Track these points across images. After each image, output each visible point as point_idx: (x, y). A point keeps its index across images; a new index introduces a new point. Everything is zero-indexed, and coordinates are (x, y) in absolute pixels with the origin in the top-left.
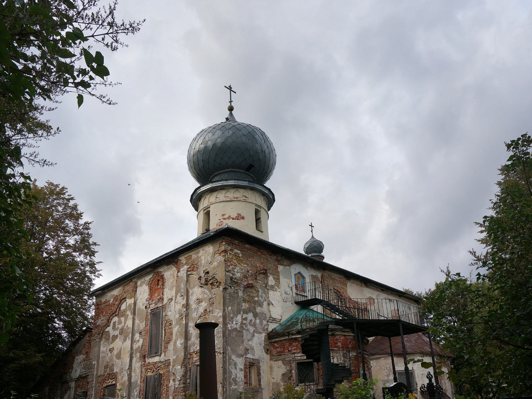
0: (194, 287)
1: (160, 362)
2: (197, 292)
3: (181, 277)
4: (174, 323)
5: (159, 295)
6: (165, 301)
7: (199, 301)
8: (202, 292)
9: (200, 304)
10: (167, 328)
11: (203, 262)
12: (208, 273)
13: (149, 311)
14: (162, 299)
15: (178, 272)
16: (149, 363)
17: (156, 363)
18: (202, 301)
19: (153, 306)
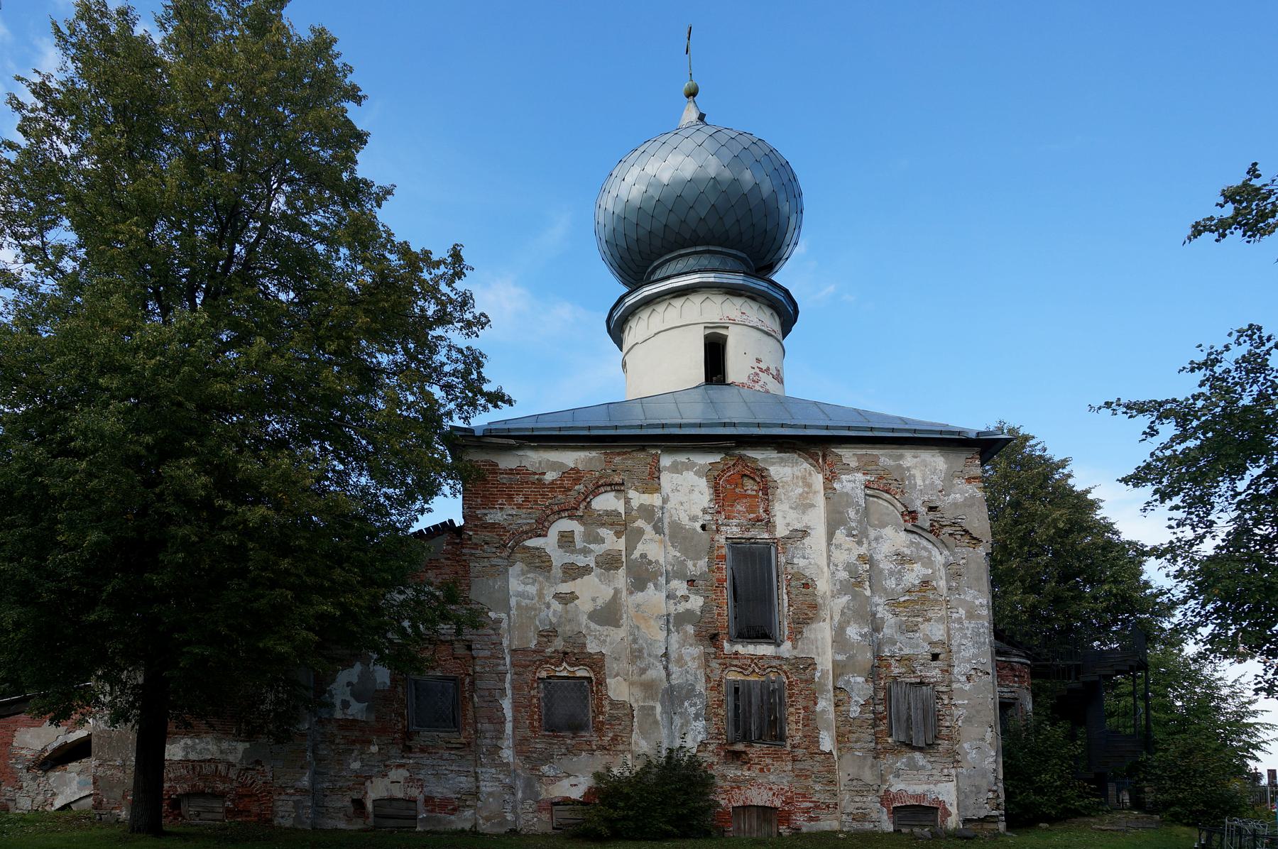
0: (883, 526)
1: (779, 658)
2: (893, 539)
3: (847, 494)
4: (823, 586)
5: (751, 509)
6: (781, 531)
7: (902, 559)
8: (912, 543)
9: (906, 566)
10: (794, 591)
11: (919, 482)
12: (932, 509)
13: (721, 539)
14: (769, 525)
15: (829, 480)
16: (736, 653)
17: (762, 657)
18: (911, 561)
19: (733, 530)
